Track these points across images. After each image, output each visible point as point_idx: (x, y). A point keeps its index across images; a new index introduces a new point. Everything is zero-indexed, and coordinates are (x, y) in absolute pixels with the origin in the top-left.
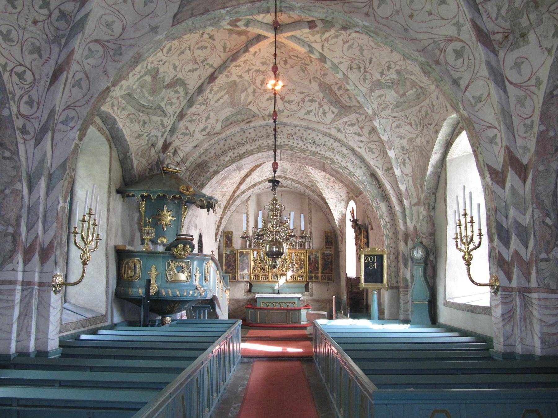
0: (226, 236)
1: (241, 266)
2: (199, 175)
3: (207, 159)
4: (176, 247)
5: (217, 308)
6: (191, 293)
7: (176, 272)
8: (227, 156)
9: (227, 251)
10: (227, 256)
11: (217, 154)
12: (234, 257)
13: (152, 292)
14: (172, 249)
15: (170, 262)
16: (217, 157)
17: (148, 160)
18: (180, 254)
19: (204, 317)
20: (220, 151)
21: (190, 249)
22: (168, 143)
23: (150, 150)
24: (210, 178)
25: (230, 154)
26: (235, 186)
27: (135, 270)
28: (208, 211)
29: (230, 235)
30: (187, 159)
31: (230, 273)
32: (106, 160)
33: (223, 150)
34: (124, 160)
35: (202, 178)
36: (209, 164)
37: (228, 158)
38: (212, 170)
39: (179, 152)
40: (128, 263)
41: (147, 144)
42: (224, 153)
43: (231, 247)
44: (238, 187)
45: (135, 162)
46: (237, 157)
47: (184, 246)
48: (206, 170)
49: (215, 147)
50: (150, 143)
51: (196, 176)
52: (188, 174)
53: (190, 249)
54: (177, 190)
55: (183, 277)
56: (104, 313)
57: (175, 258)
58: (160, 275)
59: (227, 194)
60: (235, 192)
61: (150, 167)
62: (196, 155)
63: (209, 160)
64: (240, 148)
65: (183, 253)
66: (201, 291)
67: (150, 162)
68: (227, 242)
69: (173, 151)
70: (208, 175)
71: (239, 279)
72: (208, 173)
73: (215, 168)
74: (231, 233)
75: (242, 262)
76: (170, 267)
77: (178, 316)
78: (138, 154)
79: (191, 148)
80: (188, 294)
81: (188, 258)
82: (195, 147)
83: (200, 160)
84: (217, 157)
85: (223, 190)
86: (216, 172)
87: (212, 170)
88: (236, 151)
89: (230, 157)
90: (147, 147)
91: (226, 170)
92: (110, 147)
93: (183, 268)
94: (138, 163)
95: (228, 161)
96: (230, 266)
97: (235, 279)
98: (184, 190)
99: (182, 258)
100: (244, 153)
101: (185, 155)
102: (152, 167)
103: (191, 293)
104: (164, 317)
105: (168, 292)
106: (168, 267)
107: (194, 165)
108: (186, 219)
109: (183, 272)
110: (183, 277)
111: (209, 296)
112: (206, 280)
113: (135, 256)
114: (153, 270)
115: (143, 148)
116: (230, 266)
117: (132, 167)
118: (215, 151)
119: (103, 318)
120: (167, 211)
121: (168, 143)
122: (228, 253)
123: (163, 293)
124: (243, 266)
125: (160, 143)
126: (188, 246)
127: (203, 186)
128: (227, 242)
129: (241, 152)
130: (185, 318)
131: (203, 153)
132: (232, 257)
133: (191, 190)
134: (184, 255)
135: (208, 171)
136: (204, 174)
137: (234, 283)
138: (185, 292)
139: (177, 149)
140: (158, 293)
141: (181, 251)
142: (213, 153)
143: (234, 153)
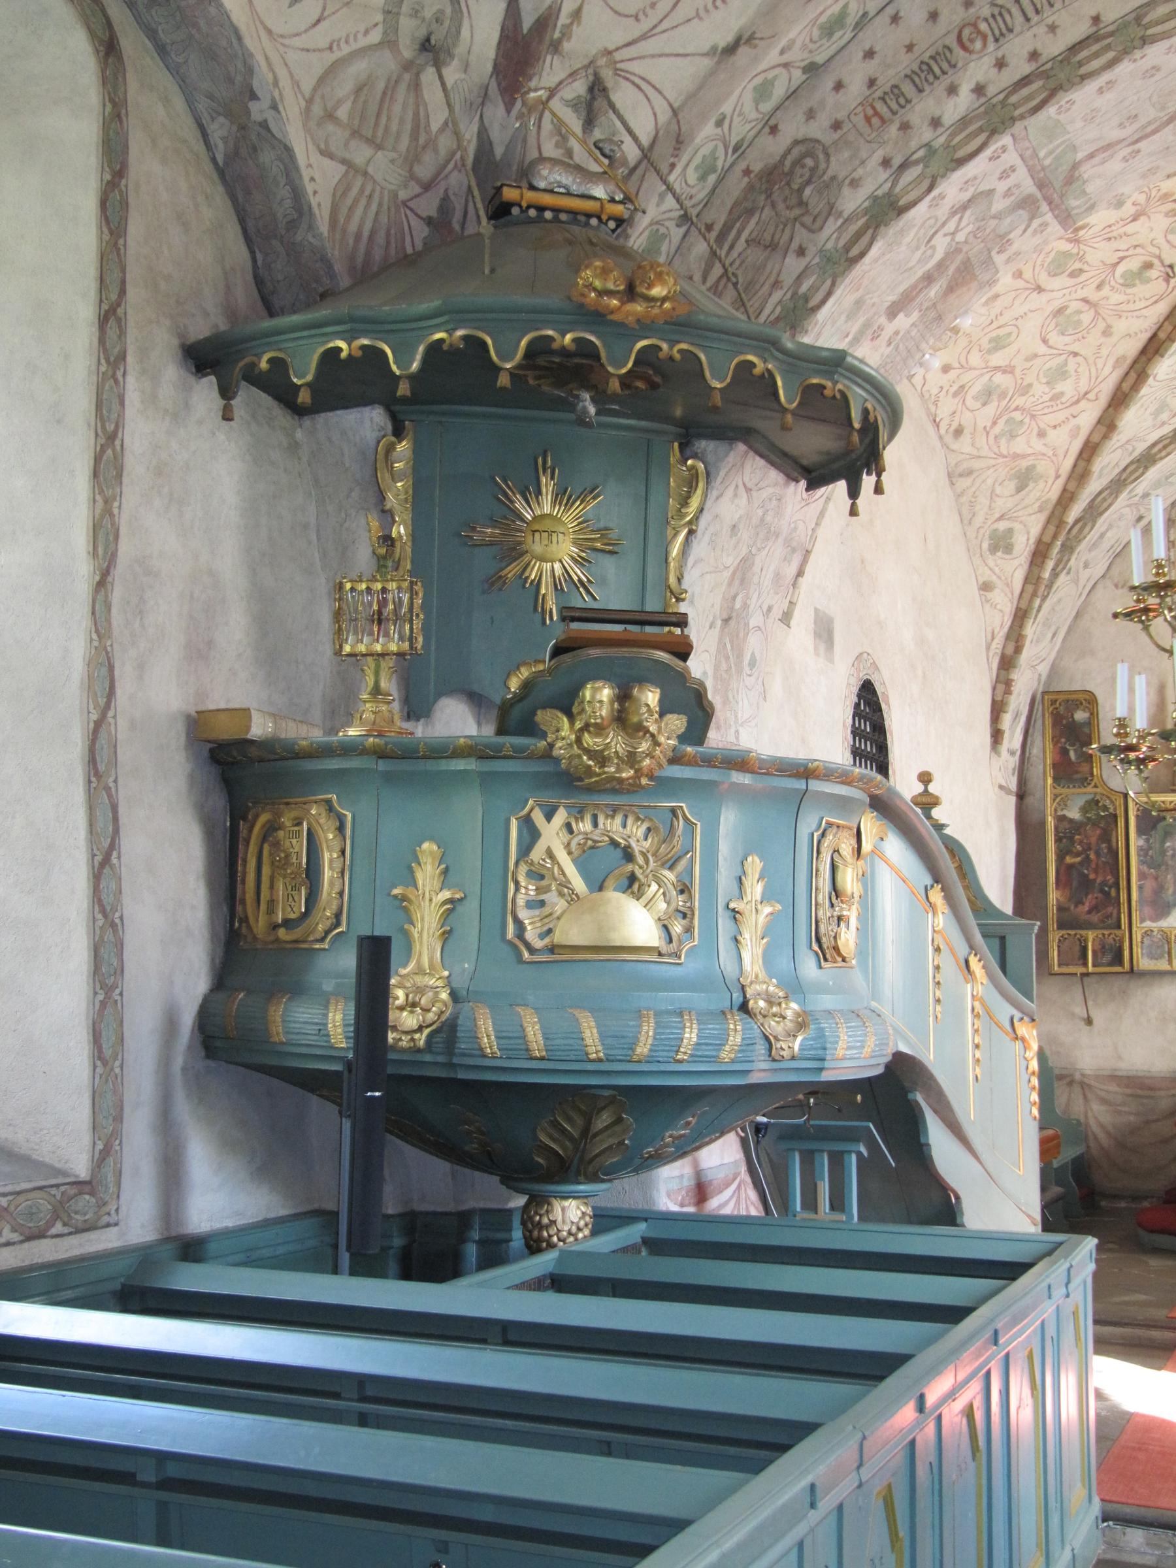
0: (1057, 719)
1: (1149, 885)
2: (772, 246)
3: (818, 130)
4: (567, 704)
5: (937, 1136)
6: (691, 1035)
7: (578, 884)
8: (952, 90)
9: (1064, 804)
10: (1068, 832)
11: (884, 84)
12: (1106, 836)
13: (407, 1023)
14: (542, 716)
15: (538, 817)
16: (887, 104)
17: (412, 159)
18: (601, 758)
19: (838, 1203)
20: (906, 62)
21: (677, 723)
22: (527, 22)
23: (416, 86)
24: (846, 258)
25: (977, 69)
26: (1088, 416)
27: (313, 873)
28: (854, 492)
29: (1080, 716)
30: (679, 142)
31: (1090, 926)
32: (78, 132)
33: (924, 50)
34: (245, 165)
35: (793, 265)
36: (837, 166)
37: (964, 101)
38: (852, 201)
39: (622, 95)
40: (272, 828)
41: (389, 42)
42: (932, 69)
43: (1085, 781)
44: (1107, 424)
45: (319, 177)
46: (1025, 81)
47: (624, 697)
48: (816, 203)
49: (867, 39)
50: (409, 30)
51: (756, 255)
52: (700, 248)
53: (677, 723)
54: (554, 301)
55: (637, 923)
56: (81, 1168)
57: (572, 784)
58: (472, 905)
59: (1043, 466)
60: (1089, 451)
61: (429, 206)
62: (740, 104)
63: (828, 137)
64: (1050, 17)
65: (616, 742)
66: (775, 1027)
67: (424, 171)
68: (1064, 752)
69: (579, 88)
70: (830, 235)
71: (1144, 963)
72: (832, 226)
73: (875, 181)
74: (1089, 701)
75: (1154, 861)
76: (537, 854)
77: (667, 1188)
78: (330, 116)
79: (707, 63)
80: (690, 1044)
81: (666, 786)
82: (731, 50)
83: (774, 147)
84: (887, 104)
85: (1019, 446)
86: (886, 210)
87: (852, 201)
88: (1017, 48)
89: (979, 90)
90: (387, 64)
91: (952, 188)
92: (108, 49)
93: (628, 856)
94: (334, 179)
95: (964, 122)
96: (1086, 885)
97: (1118, 959)
98: (602, 293)
99: (616, 787)
100: (1074, 48)
101: (664, 115)
102: (445, 206)
103: (691, 1035)
104: (538, 1201)
105: (519, 1032)
106: (525, 850)
107: (736, 185)
108: (699, 548)
109: (631, 885)
110: (637, 923)
111: (854, 1056)
112: (827, 951)
113: (308, 784)
114: (427, 874)
115: (360, 68)
116: (1086, 885)
117: (301, 208)
118: (871, 68)
119: (80, 1198)
120: (558, 498)
121: (527, 22)
122: (1074, 814)
123: (486, 1032)
124: (1160, 889)
125: (481, 35)
126: (651, 697)
127: (800, 310)
128: (1064, 752)
129: (1054, 47)
130: (737, 1200)
131: (792, 95)
132: (1094, 835)
133: (657, 291)
134: (632, 759)
135: (831, 209)
136: (801, 235)
137: (1119, 982)
138: (648, 1030)
139: (607, 75)
140: (447, 1033)
141: (600, 729)
142: (856, 88)
143: (1001, 64)
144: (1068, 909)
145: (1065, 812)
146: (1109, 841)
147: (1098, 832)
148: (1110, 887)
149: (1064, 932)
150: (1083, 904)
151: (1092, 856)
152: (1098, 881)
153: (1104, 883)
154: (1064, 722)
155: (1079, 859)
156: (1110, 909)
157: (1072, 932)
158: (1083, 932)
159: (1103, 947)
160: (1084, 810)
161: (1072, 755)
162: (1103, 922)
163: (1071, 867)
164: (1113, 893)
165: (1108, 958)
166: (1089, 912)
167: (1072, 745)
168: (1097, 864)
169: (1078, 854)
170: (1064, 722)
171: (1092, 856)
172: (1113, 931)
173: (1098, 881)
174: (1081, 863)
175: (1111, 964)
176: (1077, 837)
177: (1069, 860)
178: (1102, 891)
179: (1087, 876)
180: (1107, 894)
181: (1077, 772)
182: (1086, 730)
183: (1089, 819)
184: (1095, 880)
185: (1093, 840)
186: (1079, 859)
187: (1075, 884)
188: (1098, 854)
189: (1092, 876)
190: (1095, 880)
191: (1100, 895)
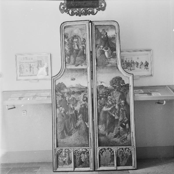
29: (111, 33)
132: (116, 95)
144: (104, 135)
146: (125, 100)
147: (120, 94)
148: (126, 124)
149: (103, 147)
150: (112, 132)
151: (117, 107)
153: (122, 121)
154: (102, 37)
155: (110, 109)
156: (126, 135)
157: (106, 148)
158: (113, 148)
159: (123, 156)
161: (106, 53)
162: (122, 142)
163: (106, 112)
165: (125, 161)
166: (115, 137)
167: (107, 49)
168: (119, 111)
170: (102, 37)
171: (117, 107)
172: (128, 147)
174: (110, 111)
175: (126, 165)
176: (109, 97)
177: (105, 109)
178: (122, 125)
179: (114, 117)
181: (109, 63)
182: (113, 41)
183: (115, 87)
185: (117, 98)
186: (110, 109)
188: (119, 105)
189: (116, 118)
190: (118, 120)
191: (121, 128)
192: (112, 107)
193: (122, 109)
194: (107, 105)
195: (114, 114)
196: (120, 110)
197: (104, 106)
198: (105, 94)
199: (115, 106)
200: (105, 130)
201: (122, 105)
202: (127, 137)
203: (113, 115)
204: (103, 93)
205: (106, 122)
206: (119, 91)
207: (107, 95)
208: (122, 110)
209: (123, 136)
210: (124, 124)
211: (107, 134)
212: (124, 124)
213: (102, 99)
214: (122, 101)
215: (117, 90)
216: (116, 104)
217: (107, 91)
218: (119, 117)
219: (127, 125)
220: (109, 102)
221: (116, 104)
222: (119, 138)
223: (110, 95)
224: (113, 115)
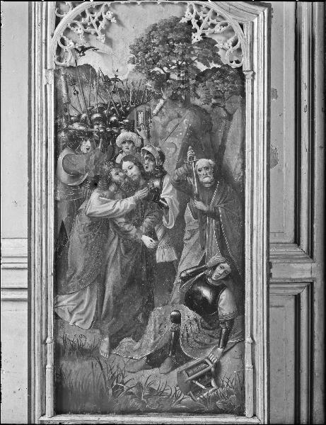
12: (207, 139)
132: (170, 126)
145: (89, 59)
146: (217, 153)
147: (187, 120)
148: (216, 291)
150: (138, 336)
152: (184, 268)
153: (199, 276)
155: (129, 202)
156: (213, 354)
160: (144, 52)
162: (192, 389)
163: (103, 225)
164: (225, 305)
166: (153, 361)
168: (180, 219)
169: (128, 188)
173: (184, 268)
174: (129, 215)
176: (124, 134)
177: (96, 204)
178: (191, 299)
179: (149, 254)
180: (206, 310)
183: (162, 81)
184: (171, 267)
185: (172, 146)
186: (129, 202)
187: (112, 277)
188: (181, 186)
189: (163, 256)
190: (171, 267)
191: (188, 314)
192: (140, 194)
193: (199, 205)
194: (110, 182)
195: (152, 234)
196: (188, 214)
197: (95, 185)
198: (104, 119)
199: (159, 190)
200: (95, 326)
201: (201, 184)
202: (218, 366)
203: (147, 240)
204: (90, 113)
205: (102, 280)
206: (186, 104)
207: (115, 124)
208: (198, 214)
209: (198, 360)
210: (206, 293)
211: (104, 348)
212: (206, 293)
213: (86, 145)
214: (202, 162)
215: (174, 98)
216: (167, 180)
217: (116, 98)
218: (179, 250)
219: (224, 295)
220: (126, 165)
221: (161, 173)
222: (174, 367)
223: (130, 127)
224: (147, 240)
